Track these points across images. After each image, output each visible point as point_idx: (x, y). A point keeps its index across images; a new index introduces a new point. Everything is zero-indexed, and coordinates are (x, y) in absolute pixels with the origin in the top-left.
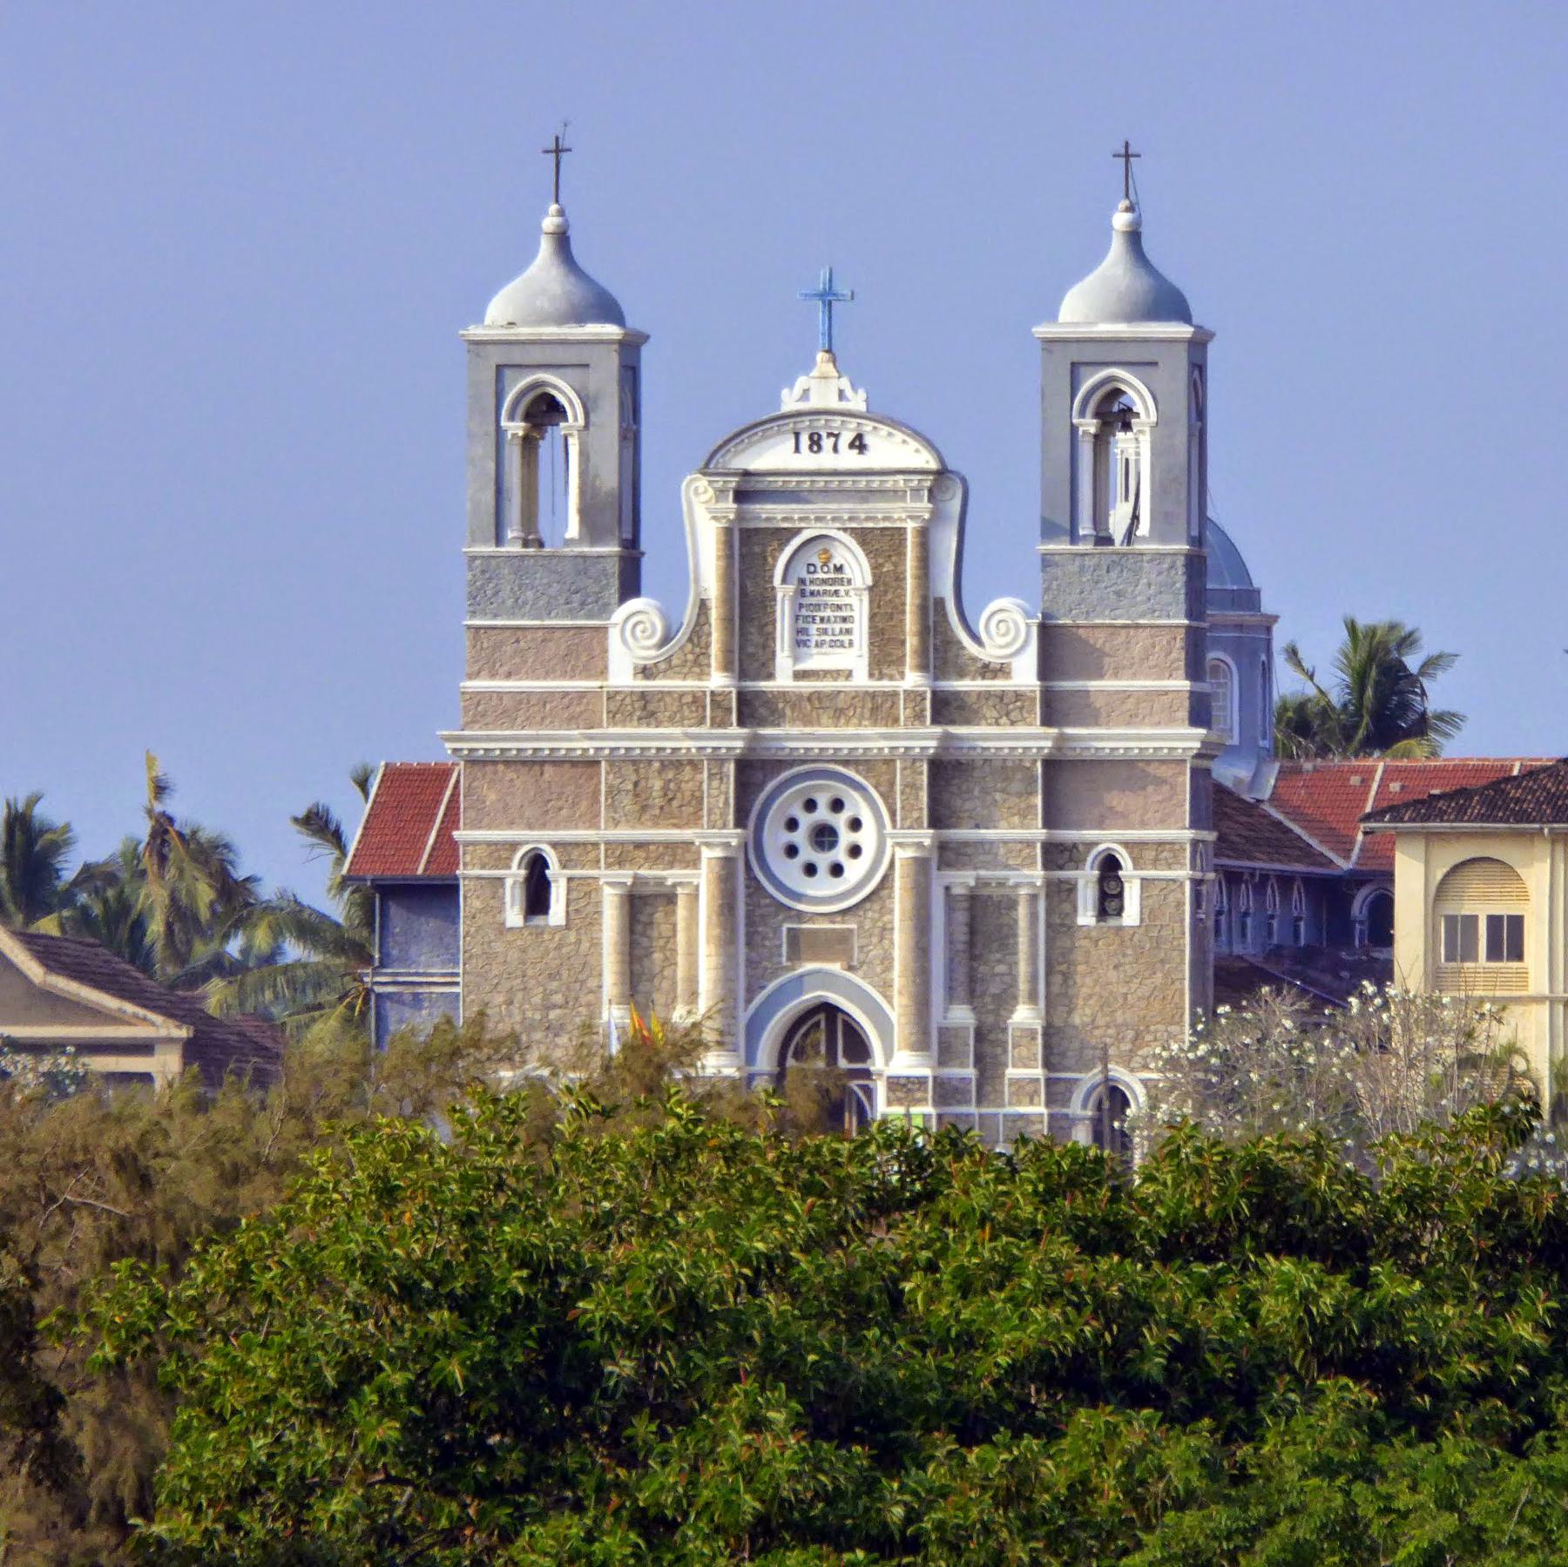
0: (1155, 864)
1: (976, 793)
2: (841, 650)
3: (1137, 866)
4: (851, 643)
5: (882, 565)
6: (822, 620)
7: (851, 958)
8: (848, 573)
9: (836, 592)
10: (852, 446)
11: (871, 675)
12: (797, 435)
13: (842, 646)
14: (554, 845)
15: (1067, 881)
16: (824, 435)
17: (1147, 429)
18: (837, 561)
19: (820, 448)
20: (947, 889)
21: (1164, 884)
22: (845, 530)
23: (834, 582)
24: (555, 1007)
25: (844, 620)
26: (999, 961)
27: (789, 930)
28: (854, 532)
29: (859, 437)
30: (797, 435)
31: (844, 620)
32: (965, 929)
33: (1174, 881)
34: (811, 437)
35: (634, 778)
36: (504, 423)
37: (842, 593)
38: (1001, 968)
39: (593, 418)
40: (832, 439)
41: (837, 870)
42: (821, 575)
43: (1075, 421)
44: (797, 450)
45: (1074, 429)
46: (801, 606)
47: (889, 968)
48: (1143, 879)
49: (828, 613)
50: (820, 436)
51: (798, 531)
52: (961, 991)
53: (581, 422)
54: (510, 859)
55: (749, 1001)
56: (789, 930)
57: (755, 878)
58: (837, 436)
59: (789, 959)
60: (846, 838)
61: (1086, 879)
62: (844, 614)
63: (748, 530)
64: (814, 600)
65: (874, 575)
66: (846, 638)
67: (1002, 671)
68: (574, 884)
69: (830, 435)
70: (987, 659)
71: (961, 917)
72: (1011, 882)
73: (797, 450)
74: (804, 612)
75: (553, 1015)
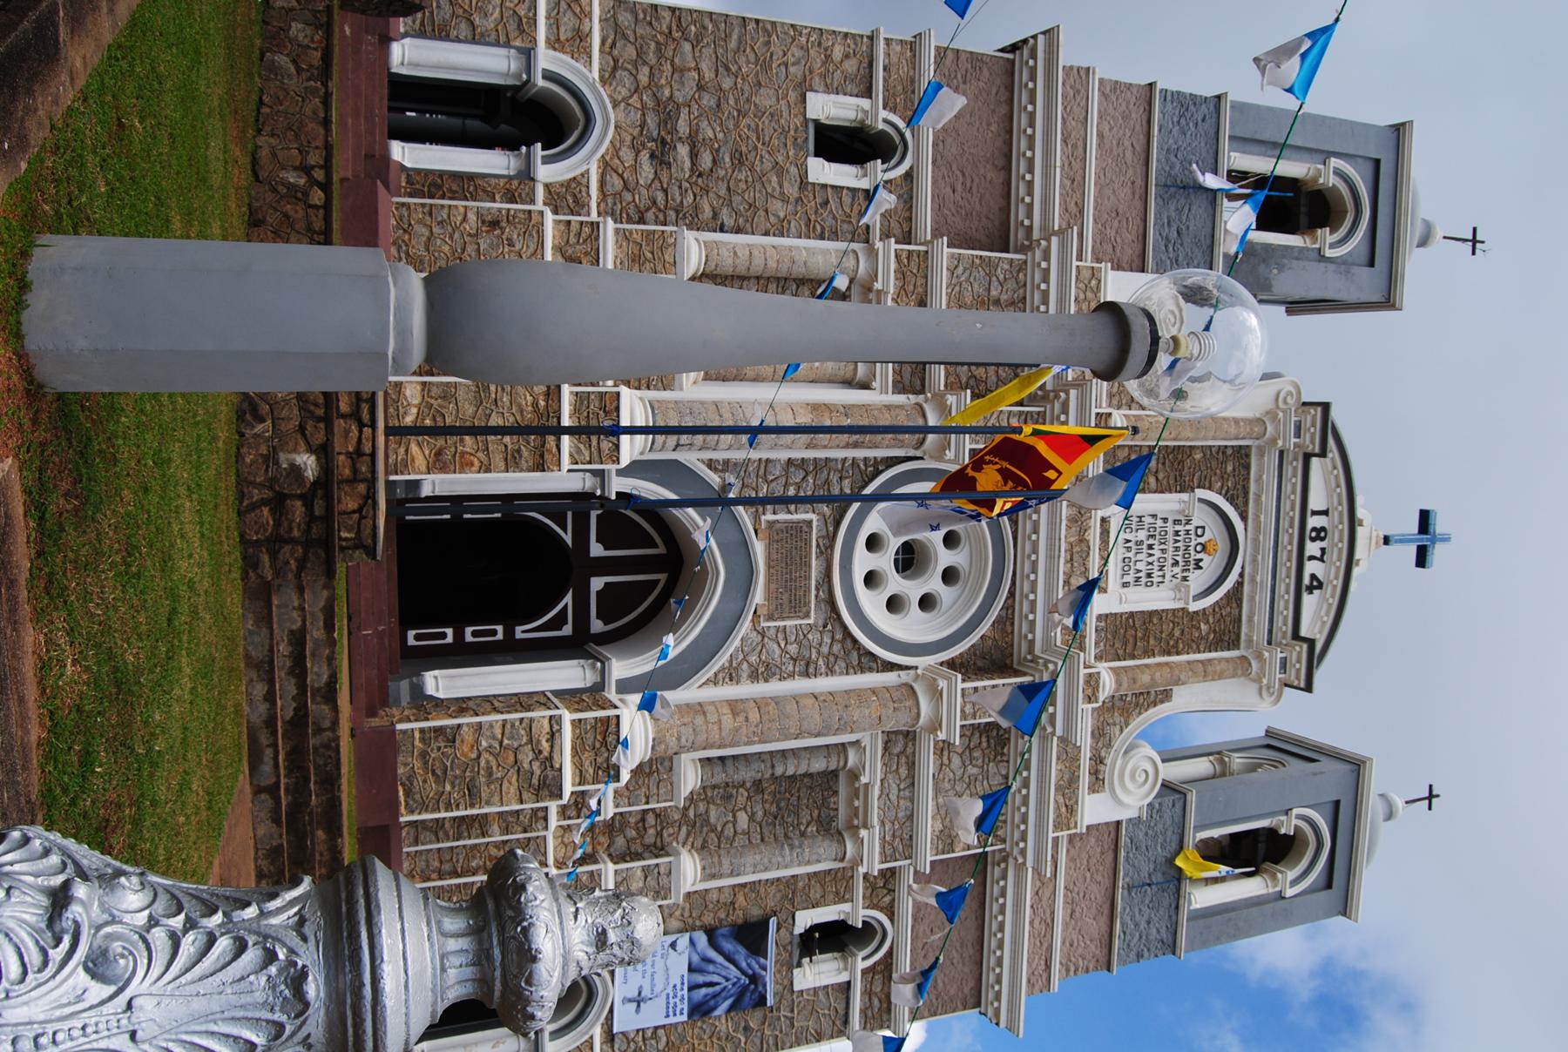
0: (868, 993)
1: (972, 770)
2: (1120, 572)
3: (864, 972)
4: (1125, 585)
5: (1207, 622)
6: (1150, 547)
7: (770, 618)
8: (1194, 576)
9: (1176, 563)
10: (1313, 577)
11: (1099, 618)
12: (1325, 513)
13: (1125, 573)
14: (908, 175)
15: (849, 888)
16: (1323, 544)
17: (1278, 889)
18: (1206, 560)
19: (1313, 540)
20: (857, 742)
21: (841, 1012)
22: (1241, 575)
23: (1187, 562)
24: (694, 155)
25: (1149, 575)
26: (752, 818)
27: (809, 523)
28: (1239, 585)
29: (1320, 586)
30: (1325, 513)
31: (1149, 575)
32: (801, 771)
33: (846, 1022)
34: (1323, 529)
35: (1004, 297)
36: (1334, 162)
37: (1177, 570)
38: (743, 818)
39: (1331, 267)
40: (1318, 554)
41: (871, 579)
42: (1193, 543)
43: (1295, 811)
44: (1314, 513)
45: (1287, 812)
46: (1165, 520)
47: (754, 676)
48: (849, 983)
49: (1157, 553)
50: (1323, 539)
51: (1244, 518)
52: (720, 778)
53: (1329, 253)
54: (894, 110)
55: (710, 464)
56: (809, 523)
57: (877, 473)
58: (1321, 559)
59: (771, 524)
60: (912, 589)
61: (856, 912)
62: (1156, 573)
63: (1248, 456)
64: (1170, 537)
65: (1196, 613)
66: (1130, 578)
67: (1097, 783)
68: (861, 196)
69: (1323, 550)
70: (1108, 761)
71: (818, 765)
72: (863, 833)
73: (1314, 513)
74: (1160, 523)
75: (683, 151)
